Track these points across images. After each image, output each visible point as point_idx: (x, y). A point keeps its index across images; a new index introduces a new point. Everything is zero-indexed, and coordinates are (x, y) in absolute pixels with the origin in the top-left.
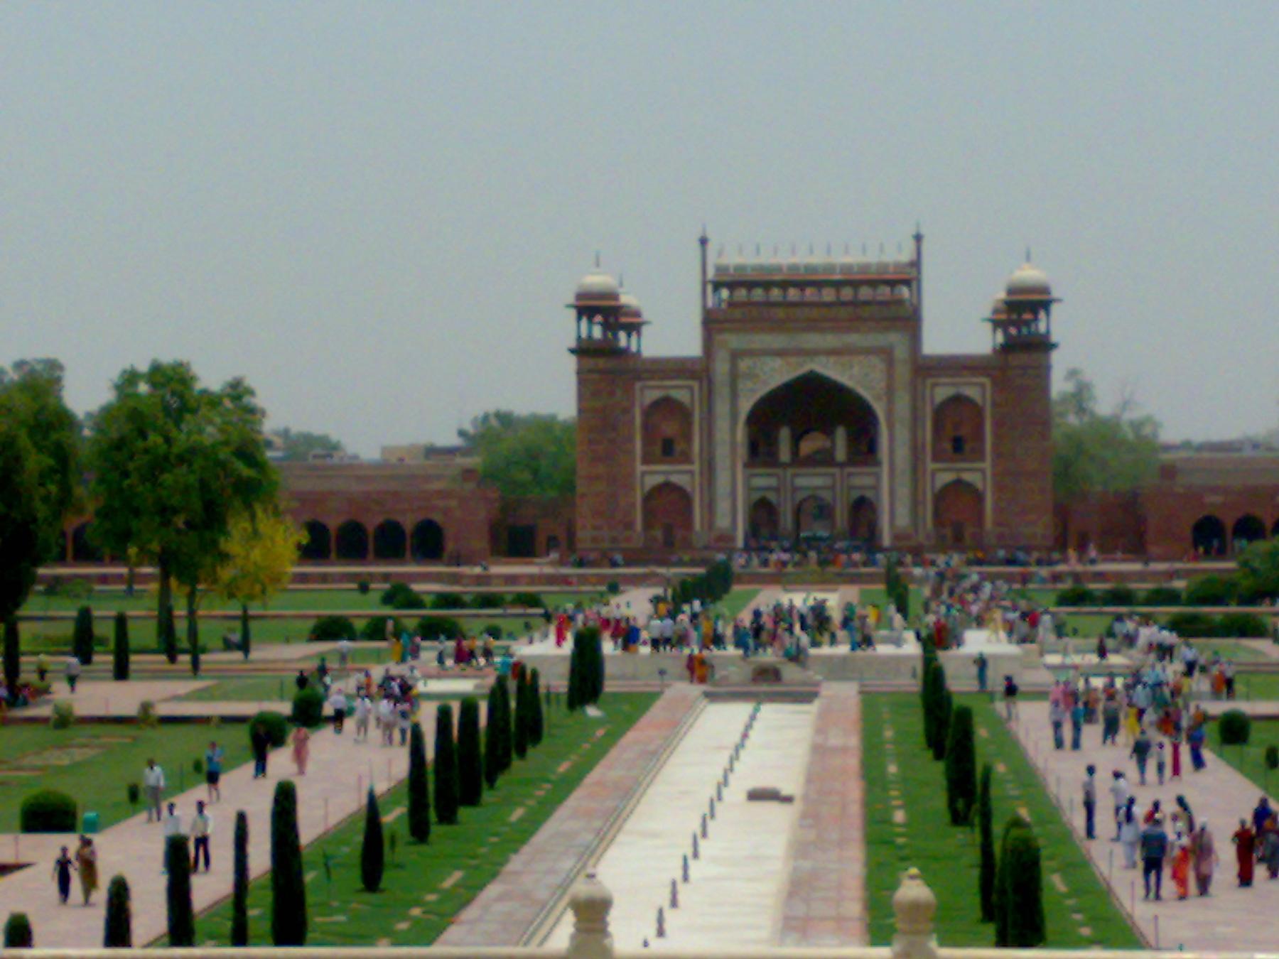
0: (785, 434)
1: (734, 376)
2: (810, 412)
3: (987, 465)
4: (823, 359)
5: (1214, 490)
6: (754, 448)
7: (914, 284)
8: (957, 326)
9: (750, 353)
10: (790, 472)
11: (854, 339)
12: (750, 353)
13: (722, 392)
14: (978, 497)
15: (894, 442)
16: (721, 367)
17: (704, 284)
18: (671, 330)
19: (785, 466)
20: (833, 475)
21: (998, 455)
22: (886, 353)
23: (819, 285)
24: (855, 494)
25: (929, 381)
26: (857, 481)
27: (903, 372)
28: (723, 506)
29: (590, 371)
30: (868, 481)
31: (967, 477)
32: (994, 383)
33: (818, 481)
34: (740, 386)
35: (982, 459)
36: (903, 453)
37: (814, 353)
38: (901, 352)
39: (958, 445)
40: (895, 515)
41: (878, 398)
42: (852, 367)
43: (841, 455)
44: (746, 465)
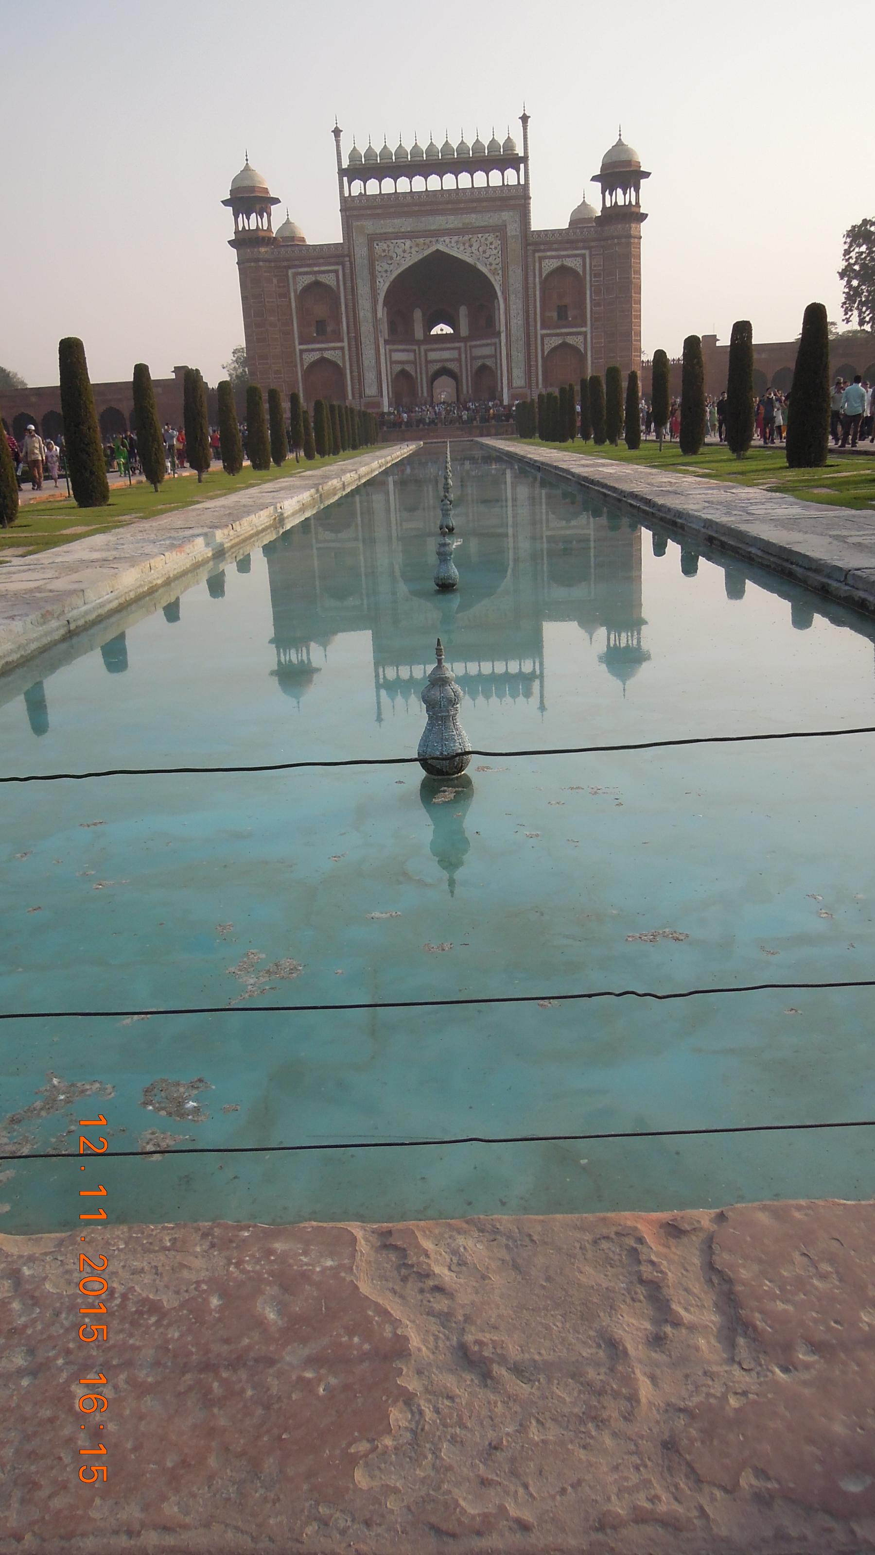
0: (418, 314)
3: (588, 329)
4: (447, 239)
6: (393, 329)
7: (522, 166)
9: (385, 237)
10: (423, 348)
11: (473, 219)
12: (385, 237)
14: (582, 357)
15: (510, 313)
16: (361, 252)
17: (342, 172)
19: (419, 343)
20: (459, 349)
21: (595, 320)
22: (500, 230)
24: (479, 363)
25: (537, 255)
26: (477, 352)
28: (370, 376)
29: (249, 260)
30: (488, 351)
31: (570, 340)
32: (591, 255)
33: (446, 355)
35: (585, 326)
36: (517, 322)
38: (513, 230)
39: (562, 312)
41: (495, 272)
42: (471, 246)
43: (464, 331)
44: (386, 342)
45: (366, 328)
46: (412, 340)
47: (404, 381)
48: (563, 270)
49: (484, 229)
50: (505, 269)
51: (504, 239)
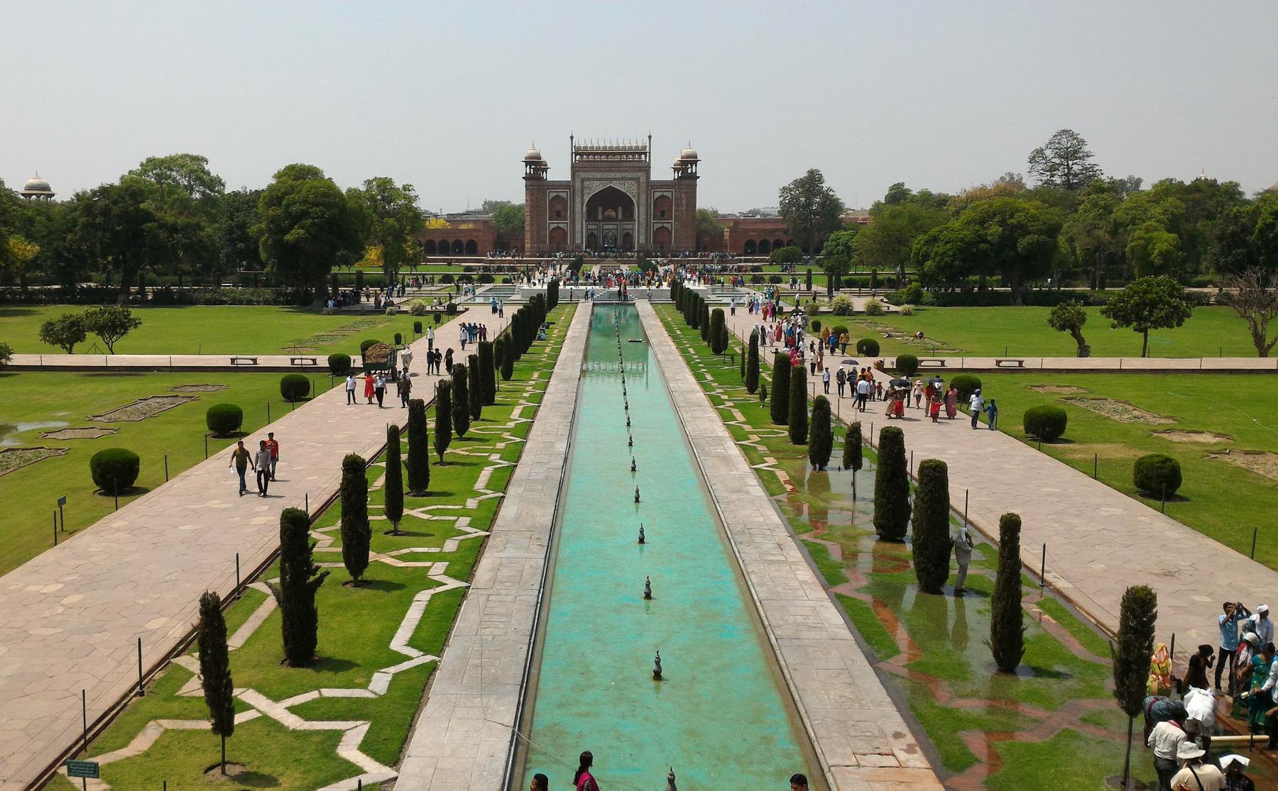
0: (600, 209)
1: (583, 188)
2: (610, 201)
5: (753, 230)
6: (589, 215)
8: (662, 170)
9: (589, 179)
11: (626, 174)
12: (589, 179)
13: (578, 194)
15: (640, 213)
16: (578, 185)
18: (559, 171)
23: (614, 154)
27: (643, 186)
28: (578, 235)
34: (586, 191)
36: (643, 217)
37: (611, 180)
40: (639, 239)
43: (620, 217)
45: (578, 216)
46: (597, 220)
47: (592, 238)
48: (663, 196)
49: (630, 179)
50: (639, 195)
51: (639, 184)
